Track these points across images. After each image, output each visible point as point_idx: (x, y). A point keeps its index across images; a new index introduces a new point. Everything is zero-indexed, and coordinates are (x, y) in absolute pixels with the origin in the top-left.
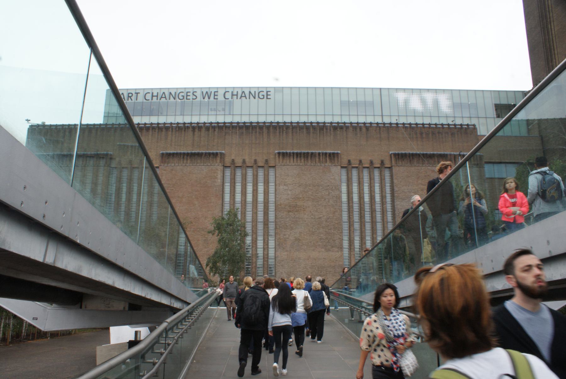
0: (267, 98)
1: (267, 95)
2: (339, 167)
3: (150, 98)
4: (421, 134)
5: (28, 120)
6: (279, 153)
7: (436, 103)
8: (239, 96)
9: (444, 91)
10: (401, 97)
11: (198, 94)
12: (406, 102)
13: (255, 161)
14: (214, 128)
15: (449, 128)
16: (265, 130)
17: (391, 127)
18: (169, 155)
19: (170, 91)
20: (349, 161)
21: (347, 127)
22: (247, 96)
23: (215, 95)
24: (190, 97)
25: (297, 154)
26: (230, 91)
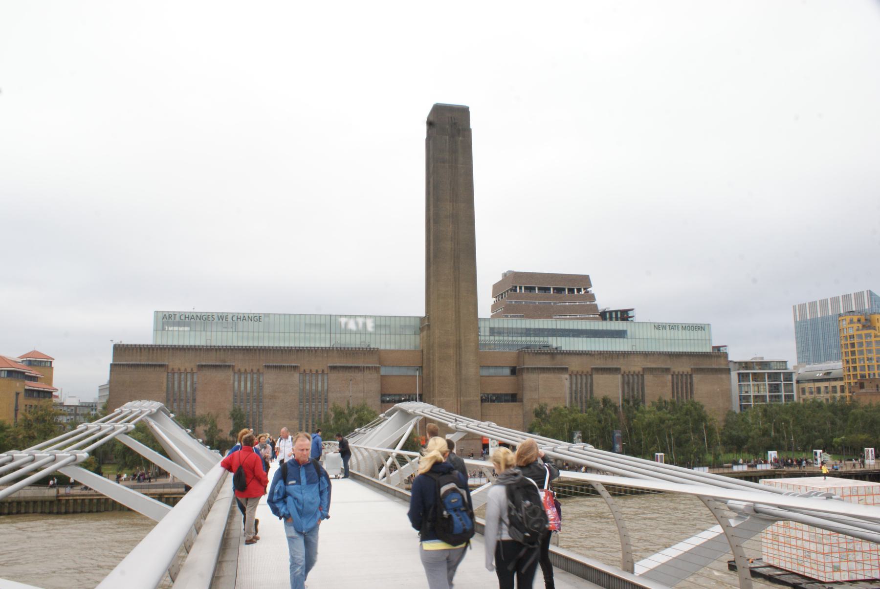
0: (259, 321)
1: (259, 319)
2: (298, 375)
3: (184, 319)
4: (346, 354)
5: (112, 341)
6: (265, 366)
7: (365, 325)
8: (241, 320)
9: (371, 316)
10: (343, 320)
11: (215, 317)
12: (346, 324)
13: (252, 370)
14: (228, 349)
15: (363, 350)
16: (257, 351)
17: (330, 350)
18: (202, 366)
19: (197, 314)
20: (304, 371)
21: (304, 350)
22: (247, 319)
23: (226, 318)
24: (210, 319)
25: (275, 366)
26: (236, 315)
